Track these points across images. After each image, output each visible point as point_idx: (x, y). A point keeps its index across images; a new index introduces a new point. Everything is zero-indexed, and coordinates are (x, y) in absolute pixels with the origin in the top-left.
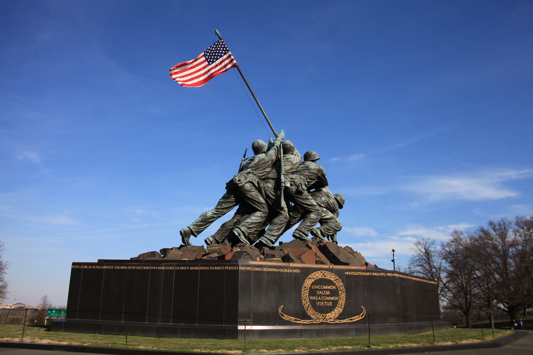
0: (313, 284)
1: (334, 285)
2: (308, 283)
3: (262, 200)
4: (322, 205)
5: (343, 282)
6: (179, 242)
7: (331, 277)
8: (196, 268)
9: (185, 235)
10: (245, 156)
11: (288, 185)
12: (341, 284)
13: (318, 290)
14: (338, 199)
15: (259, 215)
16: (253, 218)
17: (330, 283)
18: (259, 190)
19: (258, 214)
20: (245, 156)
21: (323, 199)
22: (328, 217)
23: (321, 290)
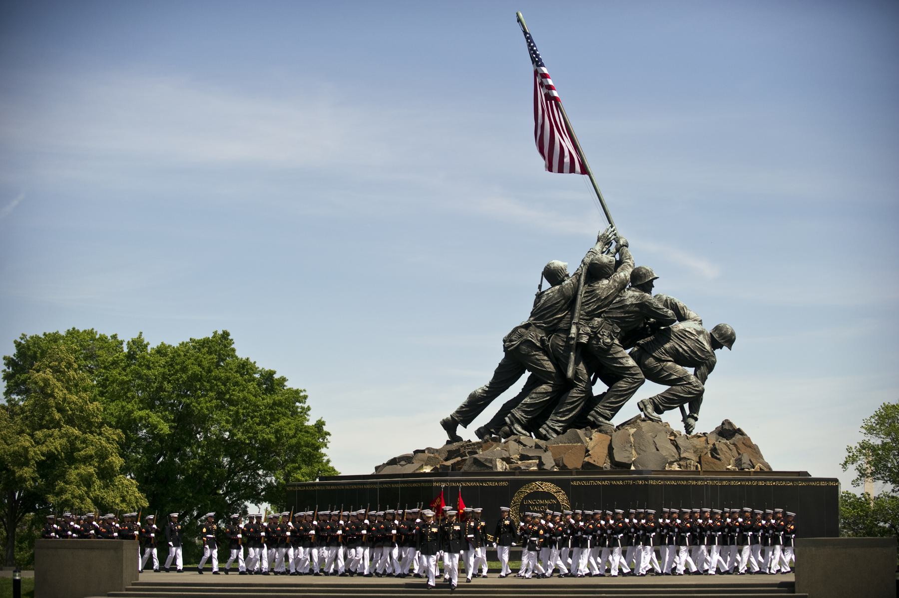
0: (526, 498)
1: (555, 498)
2: (517, 498)
3: (549, 366)
4: (664, 357)
5: (567, 493)
6: (439, 439)
7: (550, 487)
8: (397, 486)
9: (449, 426)
10: (540, 287)
11: (585, 340)
12: (565, 497)
13: (532, 505)
14: (716, 336)
15: (543, 391)
16: (533, 396)
17: (548, 495)
18: (544, 349)
19: (544, 388)
20: (540, 287)
21: (667, 346)
22: (674, 377)
23: (536, 505)
